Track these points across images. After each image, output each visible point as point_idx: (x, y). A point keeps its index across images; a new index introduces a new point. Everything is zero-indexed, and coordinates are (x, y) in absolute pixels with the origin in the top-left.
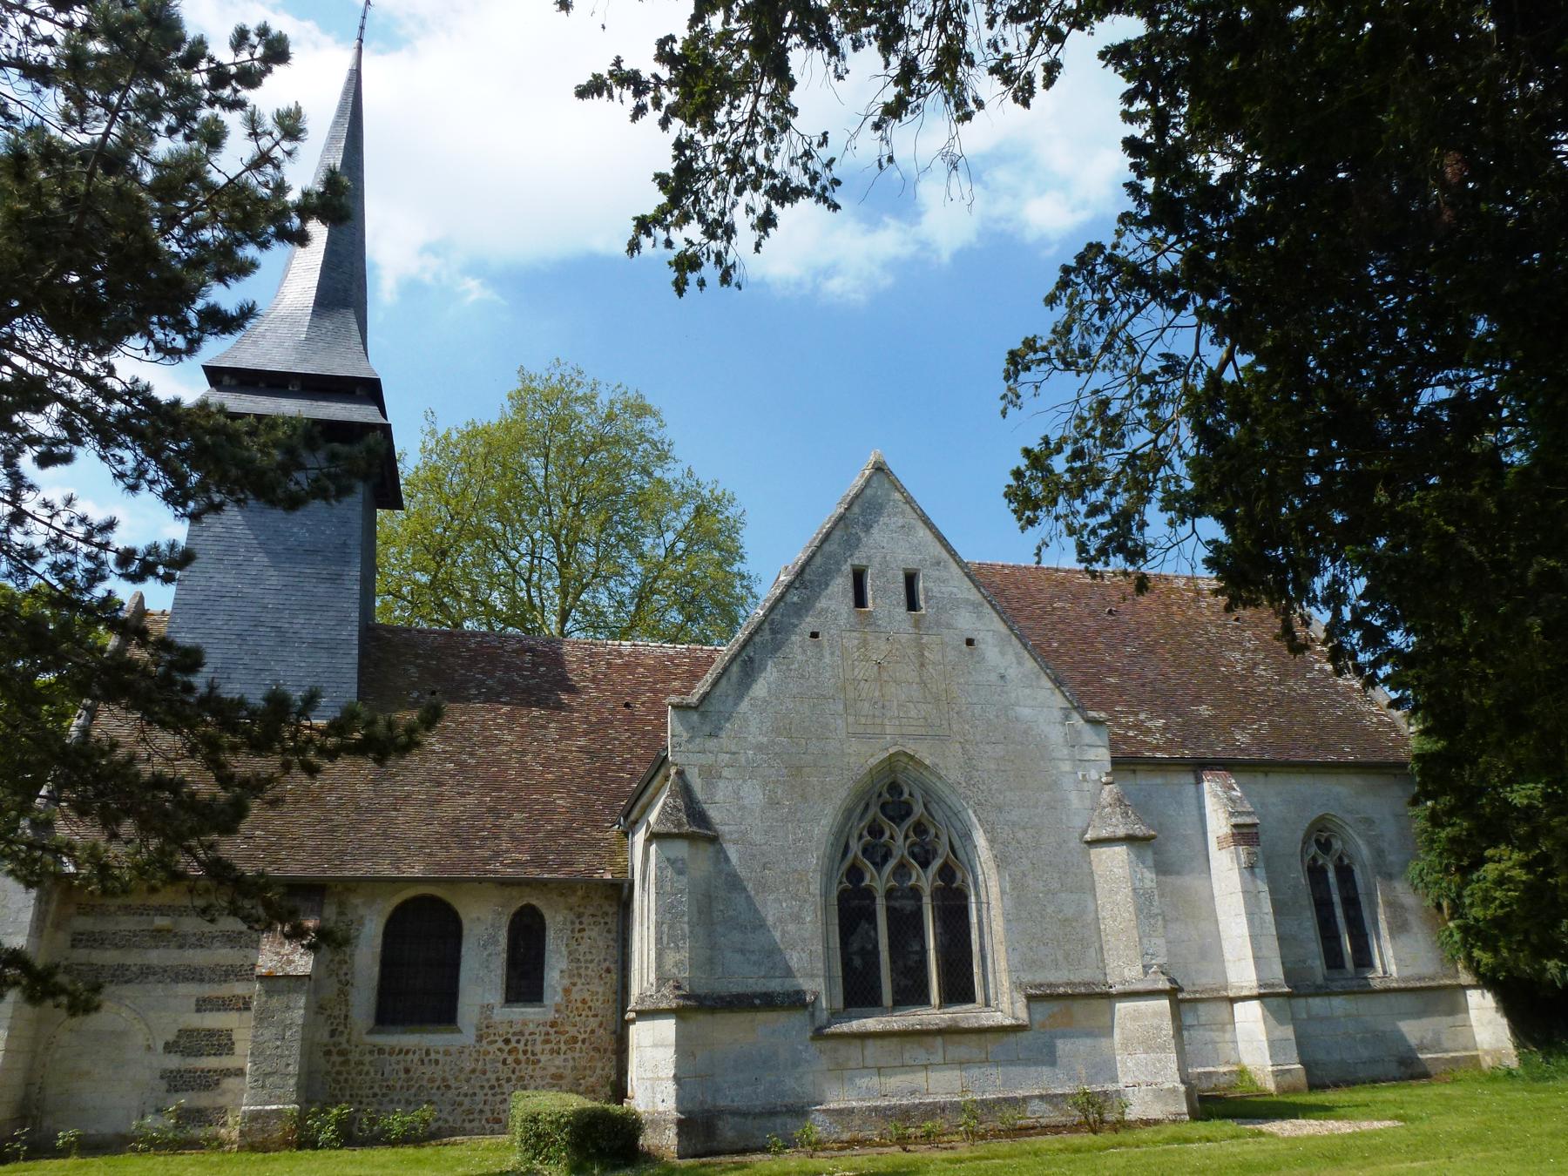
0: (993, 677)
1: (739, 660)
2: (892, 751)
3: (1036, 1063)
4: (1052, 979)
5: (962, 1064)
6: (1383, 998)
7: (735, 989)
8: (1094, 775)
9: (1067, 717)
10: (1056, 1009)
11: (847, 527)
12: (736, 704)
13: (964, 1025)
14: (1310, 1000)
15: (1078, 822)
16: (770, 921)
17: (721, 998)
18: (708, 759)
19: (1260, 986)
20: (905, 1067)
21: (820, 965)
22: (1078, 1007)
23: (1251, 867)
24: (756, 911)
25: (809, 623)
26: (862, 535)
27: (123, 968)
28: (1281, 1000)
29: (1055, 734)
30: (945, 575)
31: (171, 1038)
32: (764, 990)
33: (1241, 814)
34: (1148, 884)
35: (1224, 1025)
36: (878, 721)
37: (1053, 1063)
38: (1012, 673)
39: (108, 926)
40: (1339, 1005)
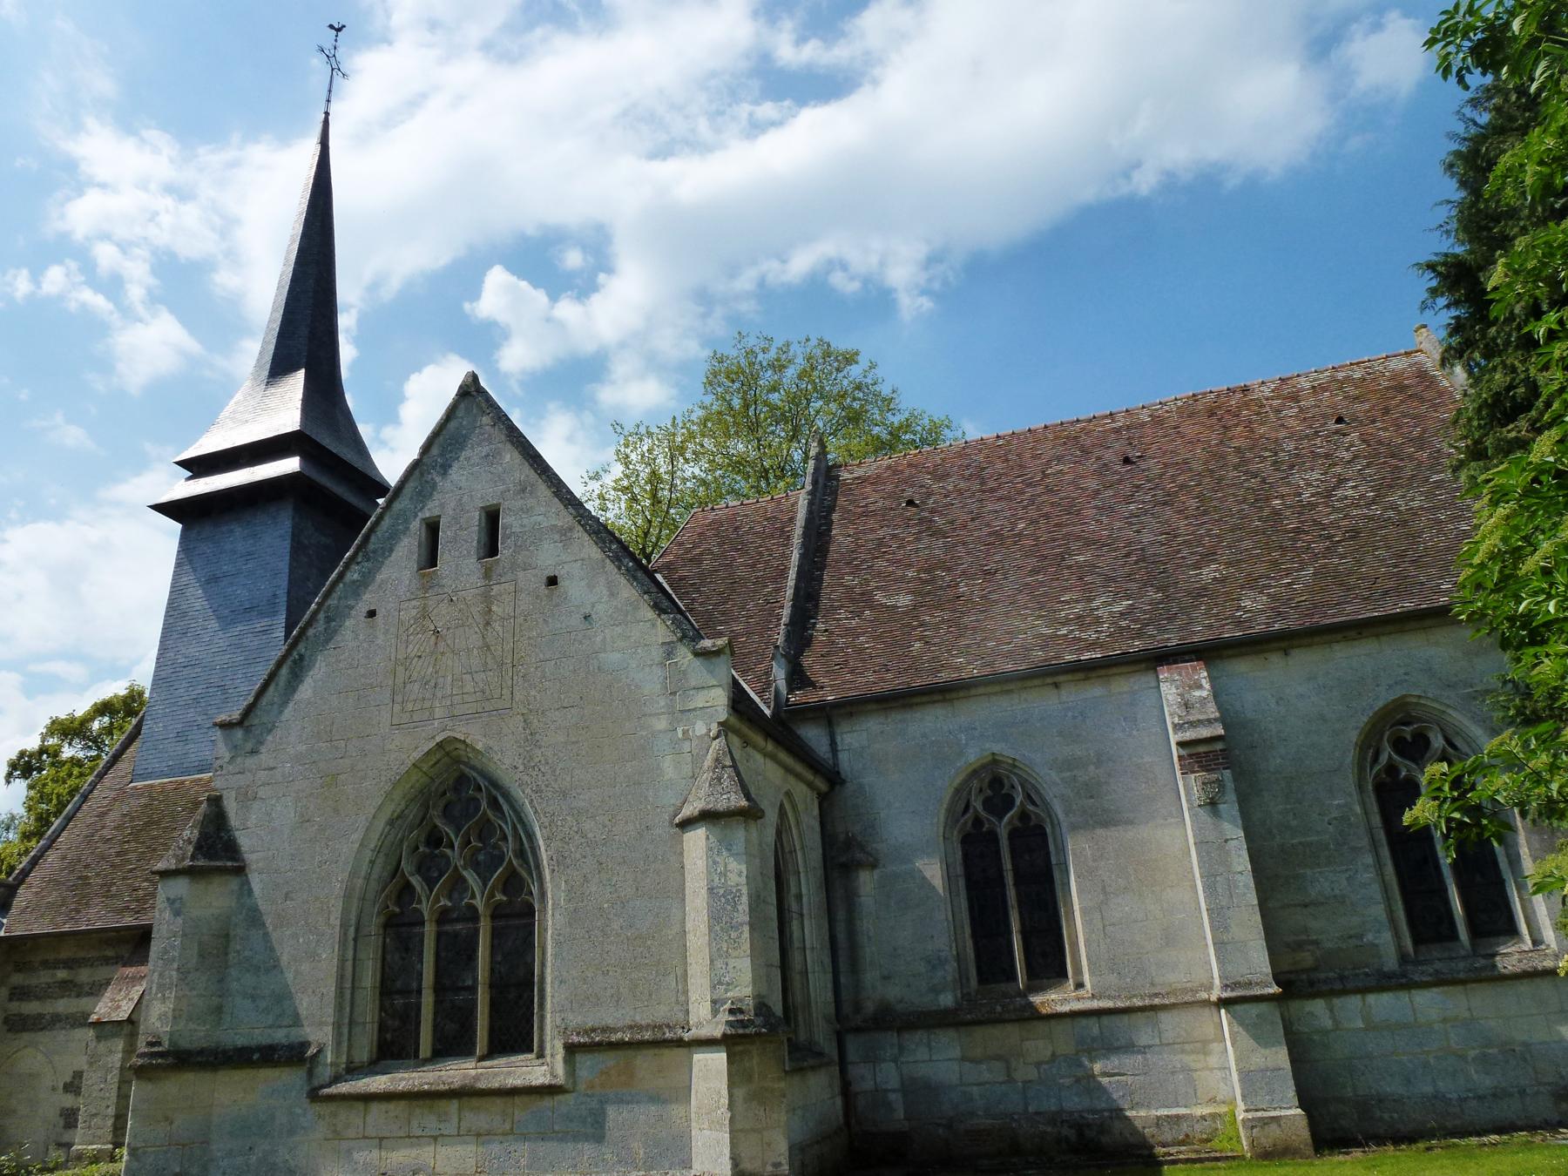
0: (576, 620)
1: (289, 662)
2: (438, 739)
3: (576, 1137)
4: (610, 1022)
5: (480, 1136)
6: (1524, 987)
7: (241, 1041)
8: (700, 728)
9: (669, 655)
10: (611, 1063)
11: (422, 475)
12: (281, 712)
13: (482, 1085)
14: (1371, 998)
15: (671, 799)
16: (285, 959)
17: (225, 1052)
18: (242, 780)
19: (1225, 987)
20: (412, 1139)
21: (331, 1011)
22: (644, 1062)
23: (1212, 804)
24: (272, 949)
25: (368, 600)
26: (438, 479)
27: (41, 1016)
28: (1263, 1007)
29: (651, 682)
30: (531, 502)
31: (68, 1079)
32: (269, 1041)
33: (1193, 724)
34: (733, 879)
35: (1205, 1042)
36: (427, 704)
37: (599, 1138)
38: (602, 610)
39: (33, 981)
40: (1428, 1003)
